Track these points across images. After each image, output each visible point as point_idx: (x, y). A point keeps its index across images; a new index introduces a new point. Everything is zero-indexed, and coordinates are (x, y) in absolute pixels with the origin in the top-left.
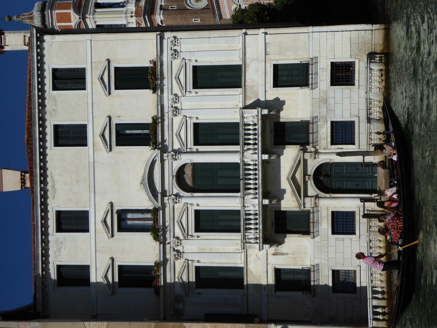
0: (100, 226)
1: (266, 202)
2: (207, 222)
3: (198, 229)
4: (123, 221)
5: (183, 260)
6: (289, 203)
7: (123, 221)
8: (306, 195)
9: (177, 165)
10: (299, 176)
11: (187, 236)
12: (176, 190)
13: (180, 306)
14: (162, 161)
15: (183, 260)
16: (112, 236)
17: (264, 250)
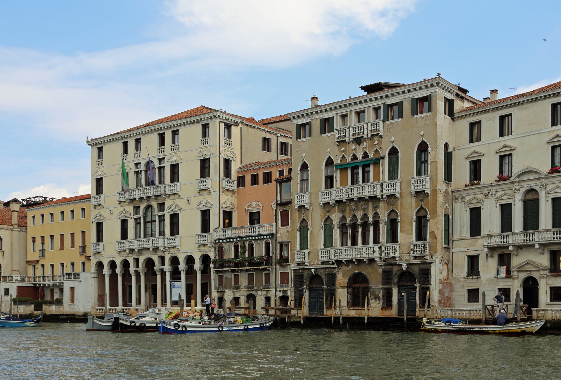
0: (502, 144)
1: (511, 248)
2: (506, 210)
3: (502, 206)
4: (505, 158)
5: (483, 198)
6: (515, 262)
7: (505, 158)
8: (518, 271)
9: (537, 188)
10: (528, 267)
11: (497, 200)
12: (523, 190)
13: (460, 200)
14: (539, 179)
15: (483, 198)
16: (497, 153)
17: (483, 249)
